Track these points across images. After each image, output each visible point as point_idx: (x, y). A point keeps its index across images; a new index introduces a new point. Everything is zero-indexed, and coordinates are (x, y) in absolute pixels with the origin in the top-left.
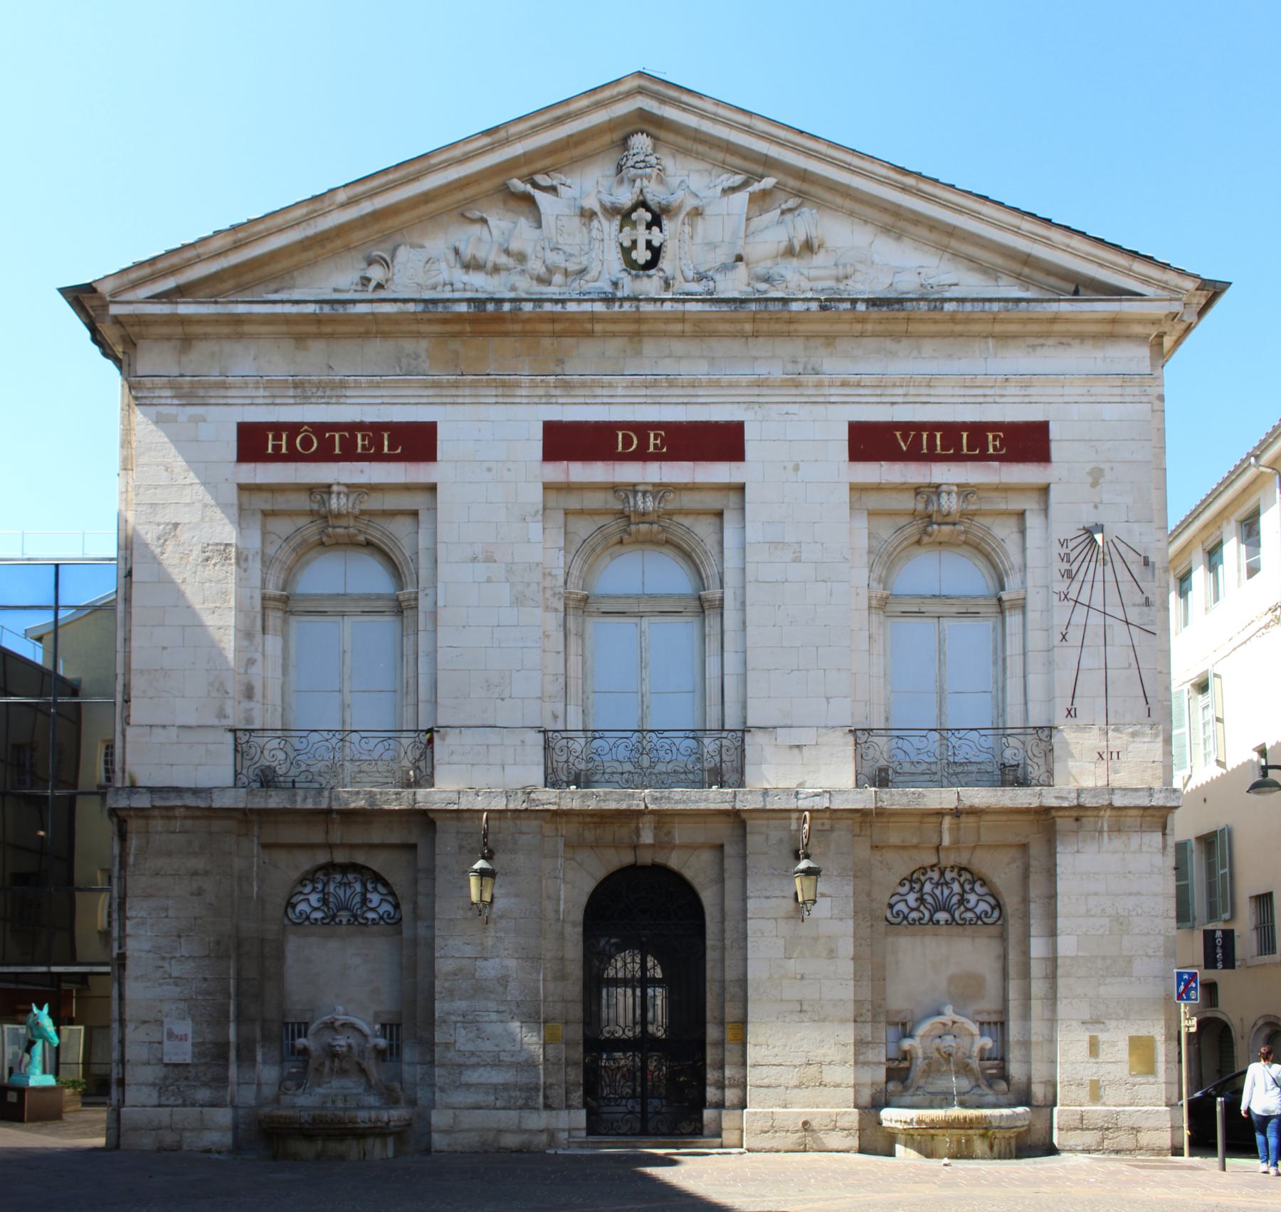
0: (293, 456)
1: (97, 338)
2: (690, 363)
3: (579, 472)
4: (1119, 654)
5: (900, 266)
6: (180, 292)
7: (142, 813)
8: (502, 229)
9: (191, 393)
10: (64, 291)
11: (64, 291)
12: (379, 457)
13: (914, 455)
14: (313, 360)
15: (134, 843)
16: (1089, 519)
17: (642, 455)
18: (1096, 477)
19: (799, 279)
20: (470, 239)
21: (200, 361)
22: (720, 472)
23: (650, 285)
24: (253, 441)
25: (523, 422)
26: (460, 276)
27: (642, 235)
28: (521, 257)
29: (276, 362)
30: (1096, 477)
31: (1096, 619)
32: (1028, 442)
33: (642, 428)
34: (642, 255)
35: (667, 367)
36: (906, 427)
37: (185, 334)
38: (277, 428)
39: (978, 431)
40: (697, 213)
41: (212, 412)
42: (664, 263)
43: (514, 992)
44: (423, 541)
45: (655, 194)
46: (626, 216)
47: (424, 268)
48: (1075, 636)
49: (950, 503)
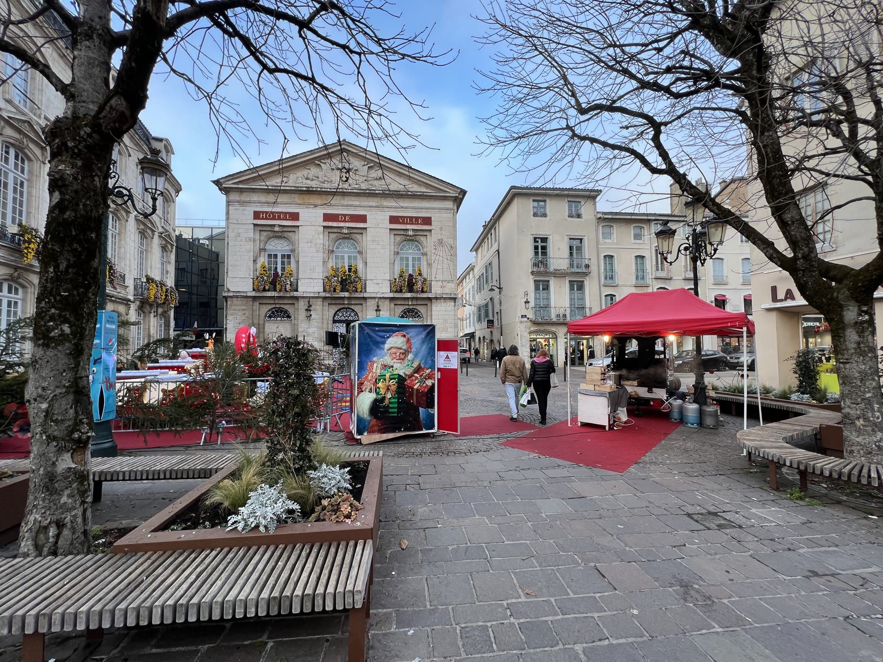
0: (266, 219)
1: (220, 189)
2: (355, 201)
3: (330, 224)
4: (446, 266)
5: (396, 184)
6: (240, 182)
7: (231, 297)
8: (313, 171)
9: (242, 203)
10: (214, 182)
11: (214, 182)
12: (286, 219)
13: (403, 223)
14: (271, 198)
15: (229, 303)
16: (440, 237)
17: (345, 221)
18: (441, 229)
19: (379, 186)
20: (305, 172)
21: (245, 197)
22: (362, 225)
23: (346, 186)
24: (257, 215)
25: (320, 212)
26: (305, 181)
27: (344, 175)
28: (318, 177)
29: (263, 198)
30: (441, 229)
31: (441, 258)
32: (427, 221)
33: (345, 215)
34: (344, 179)
35: (350, 203)
36: (401, 217)
37: (241, 191)
38: (263, 212)
39: (417, 218)
40: (356, 170)
41: (248, 208)
42: (350, 181)
43: (316, 335)
44: (297, 238)
45: (347, 166)
46: (341, 170)
47: (296, 179)
48: (436, 262)
49: (411, 233)
